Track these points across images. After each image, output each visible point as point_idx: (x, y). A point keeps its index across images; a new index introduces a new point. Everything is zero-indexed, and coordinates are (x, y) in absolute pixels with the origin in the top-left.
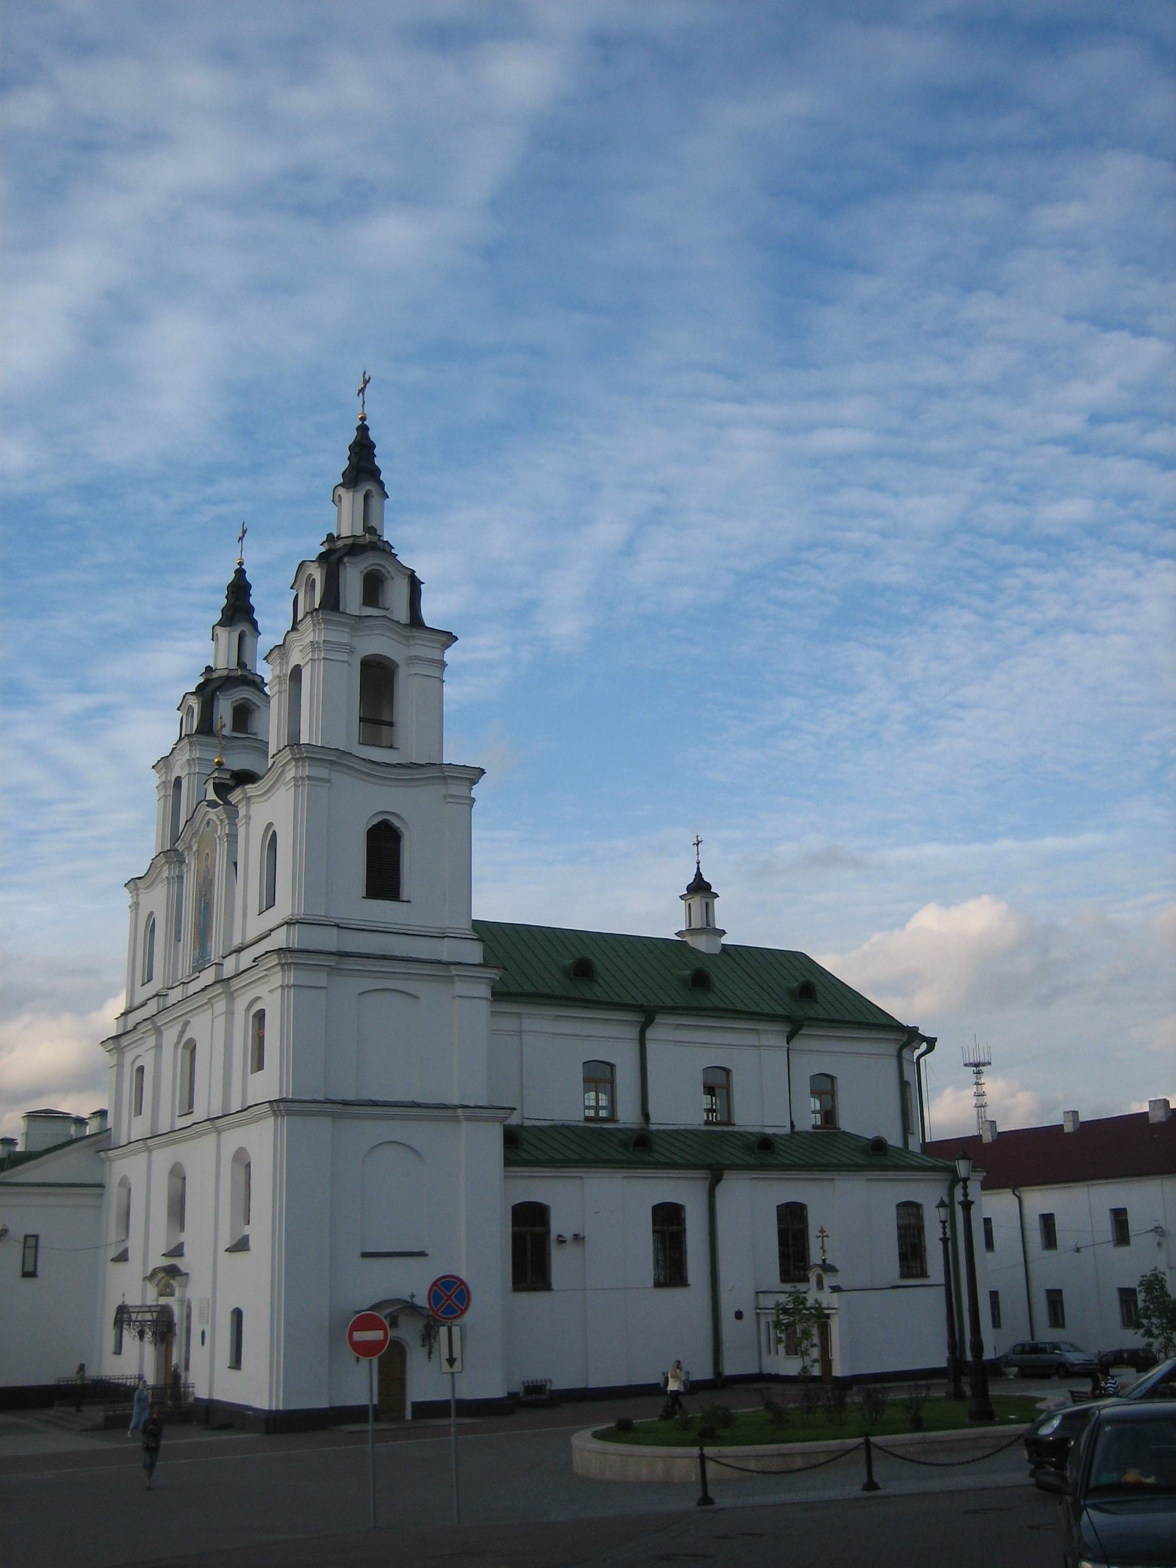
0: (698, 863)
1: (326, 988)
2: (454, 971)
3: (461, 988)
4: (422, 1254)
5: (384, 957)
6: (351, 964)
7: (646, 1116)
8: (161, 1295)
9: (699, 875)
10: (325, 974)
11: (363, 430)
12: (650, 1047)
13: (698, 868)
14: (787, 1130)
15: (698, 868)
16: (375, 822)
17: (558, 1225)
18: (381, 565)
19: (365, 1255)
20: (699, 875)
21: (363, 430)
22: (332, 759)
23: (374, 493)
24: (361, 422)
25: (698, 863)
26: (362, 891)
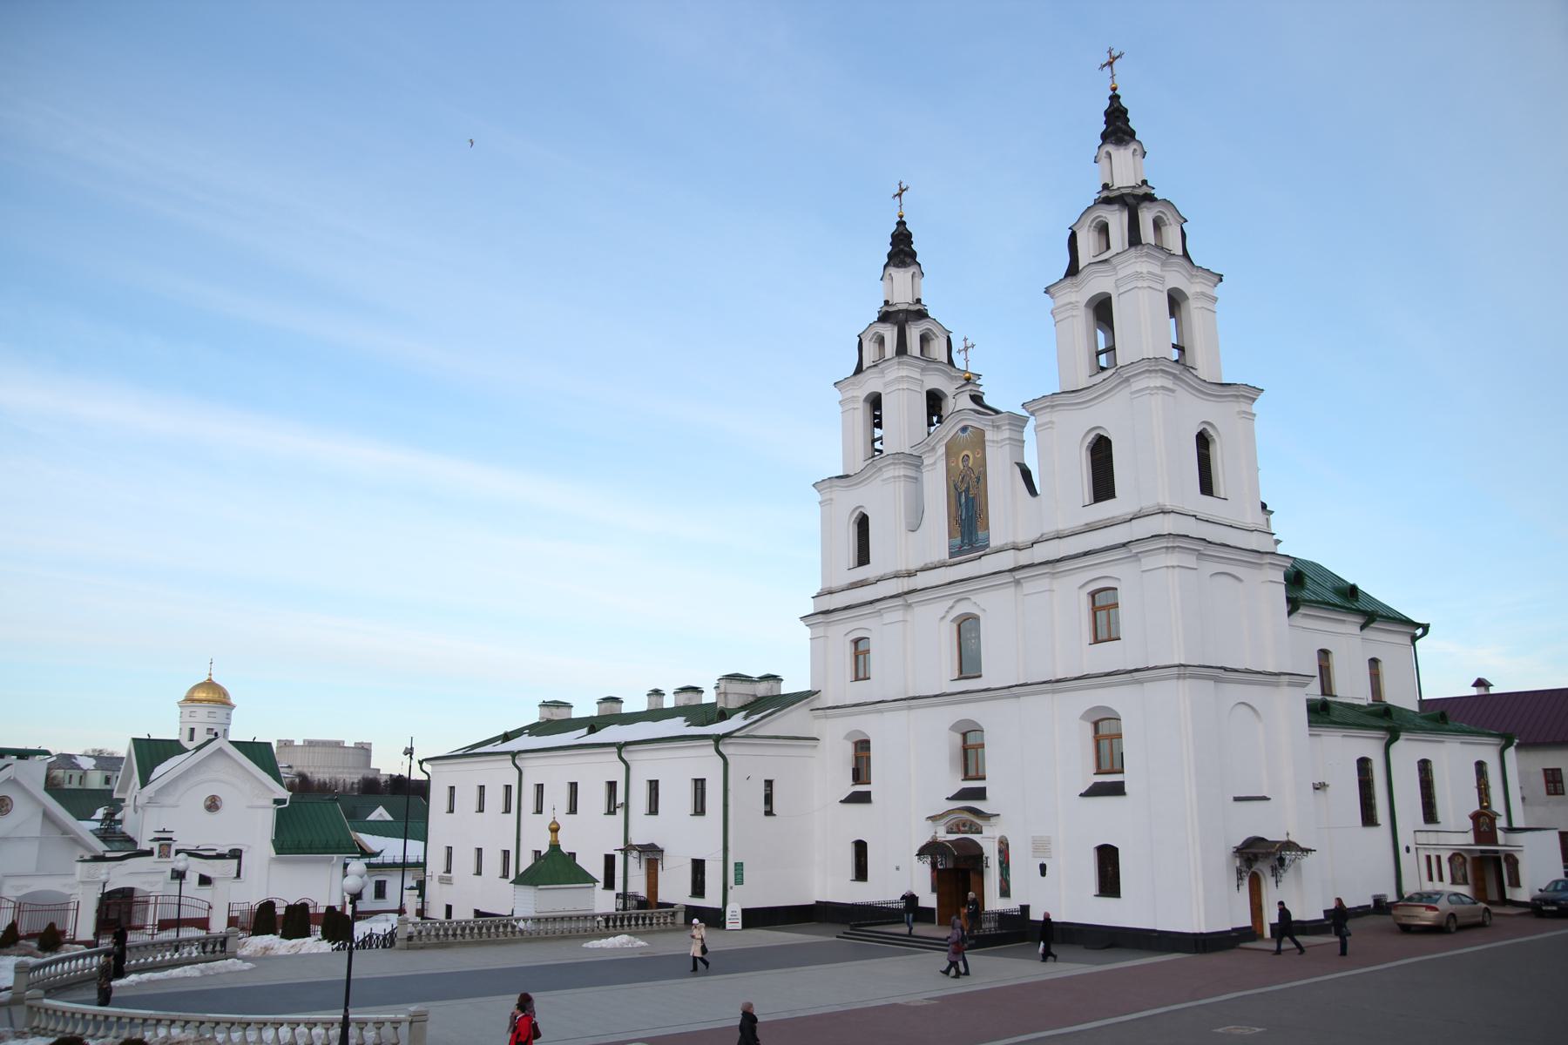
1: (1196, 569)
2: (1135, 549)
5: (1086, 554)
6: (1211, 551)
8: (948, 833)
10: (1195, 557)
11: (1115, 98)
19: (1237, 799)
21: (1115, 98)
22: (1174, 371)
23: (1111, 151)
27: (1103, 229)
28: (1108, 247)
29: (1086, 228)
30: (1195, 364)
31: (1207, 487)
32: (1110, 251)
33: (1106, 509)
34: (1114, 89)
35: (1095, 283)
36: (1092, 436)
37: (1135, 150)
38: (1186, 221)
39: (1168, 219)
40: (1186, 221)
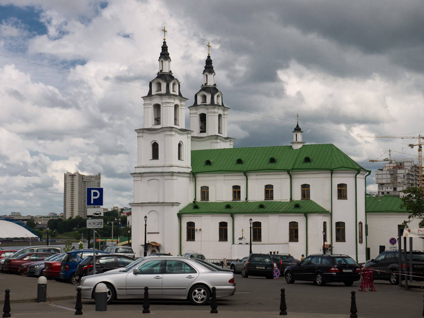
0: (298, 122)
3: (166, 177)
4: (159, 233)
5: (151, 173)
7: (246, 199)
9: (298, 126)
12: (249, 181)
13: (298, 124)
14: (289, 200)
15: (298, 124)
16: (153, 143)
17: (197, 227)
18: (158, 81)
20: (298, 126)
21: (165, 43)
24: (164, 41)
25: (298, 122)
26: (151, 157)
27: (159, 85)
28: (161, 91)
29: (155, 83)
30: (179, 124)
31: (179, 158)
32: (161, 92)
33: (155, 162)
34: (164, 40)
35: (157, 101)
36: (153, 142)
37: (169, 61)
38: (180, 83)
39: (176, 83)
40: (180, 83)
